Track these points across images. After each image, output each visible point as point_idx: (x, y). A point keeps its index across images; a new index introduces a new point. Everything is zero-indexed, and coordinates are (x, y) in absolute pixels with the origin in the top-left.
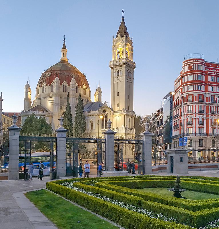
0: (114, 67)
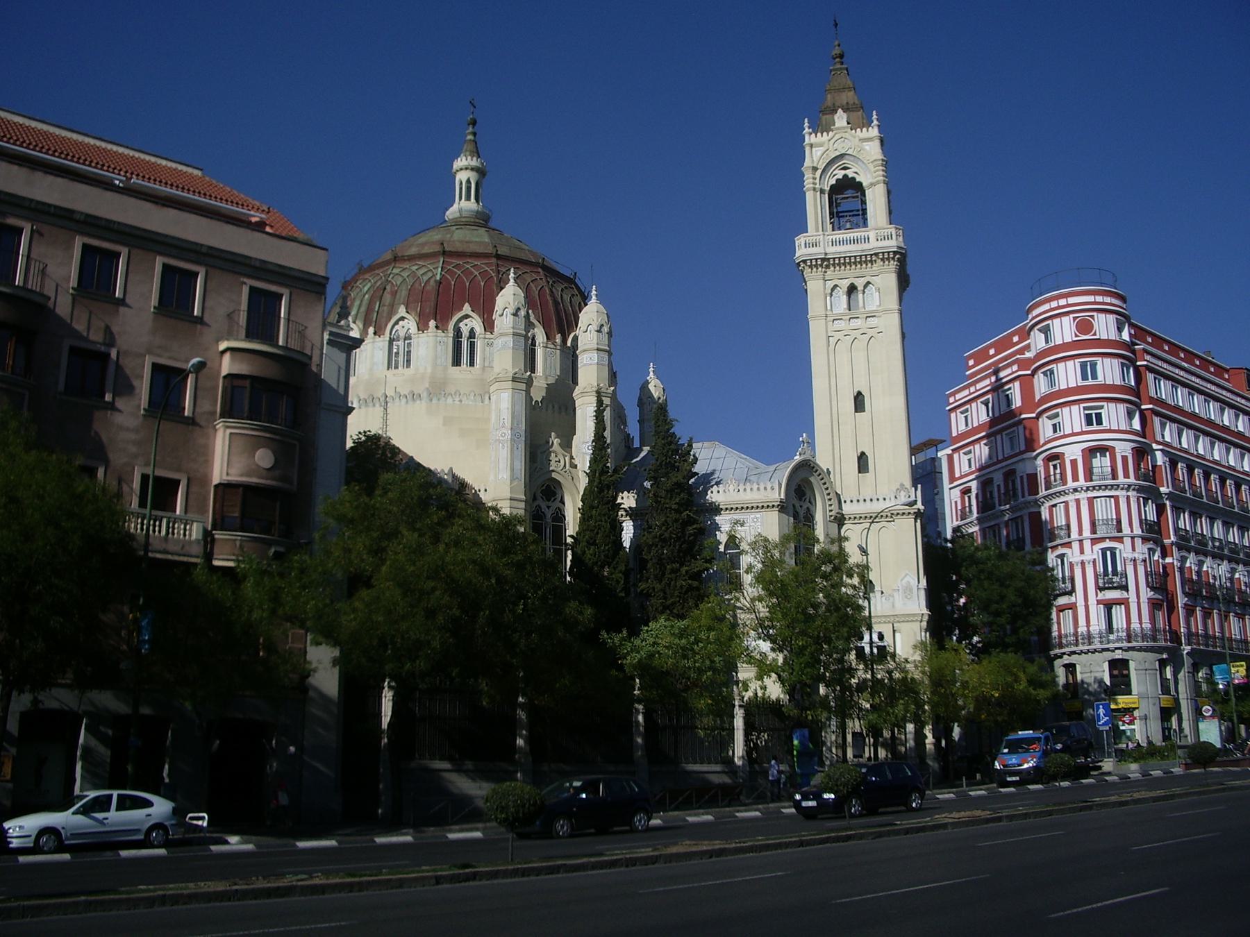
0: (828, 267)
